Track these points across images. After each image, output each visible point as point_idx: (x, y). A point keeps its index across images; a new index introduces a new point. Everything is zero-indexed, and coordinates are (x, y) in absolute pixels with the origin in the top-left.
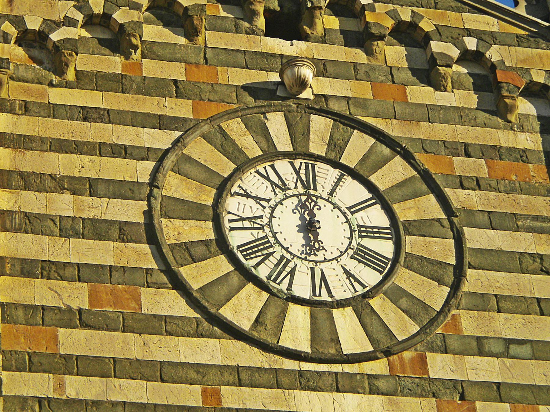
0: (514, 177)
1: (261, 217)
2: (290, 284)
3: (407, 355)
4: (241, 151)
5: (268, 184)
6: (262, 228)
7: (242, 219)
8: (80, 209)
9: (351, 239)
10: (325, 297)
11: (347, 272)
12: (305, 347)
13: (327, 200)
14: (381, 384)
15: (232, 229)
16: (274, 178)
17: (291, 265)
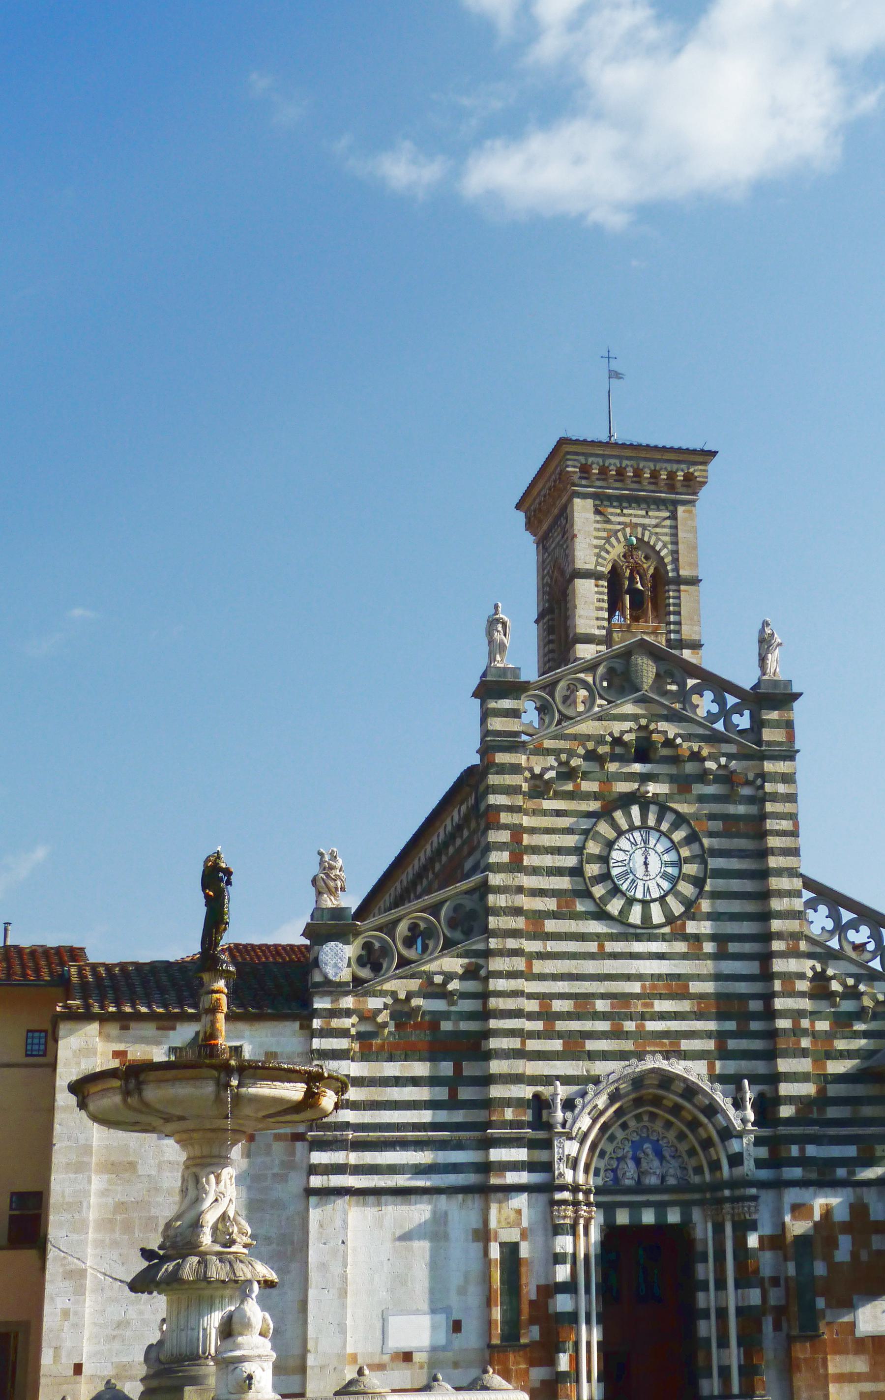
0: (734, 830)
1: (626, 860)
2: (635, 893)
3: (679, 922)
4: (619, 827)
5: (629, 843)
6: (625, 866)
7: (618, 862)
8: (554, 863)
9: (661, 868)
10: (648, 898)
11: (658, 885)
12: (638, 922)
13: (653, 849)
14: (667, 937)
15: (614, 867)
16: (632, 840)
17: (636, 883)
